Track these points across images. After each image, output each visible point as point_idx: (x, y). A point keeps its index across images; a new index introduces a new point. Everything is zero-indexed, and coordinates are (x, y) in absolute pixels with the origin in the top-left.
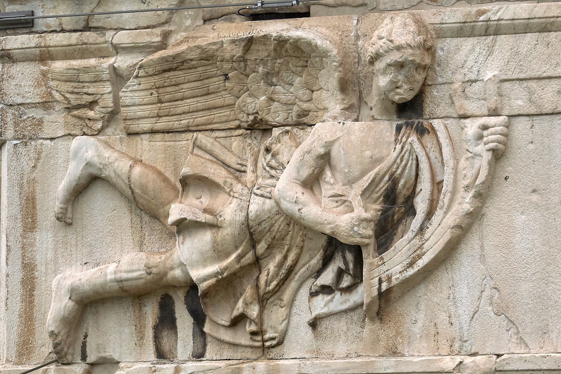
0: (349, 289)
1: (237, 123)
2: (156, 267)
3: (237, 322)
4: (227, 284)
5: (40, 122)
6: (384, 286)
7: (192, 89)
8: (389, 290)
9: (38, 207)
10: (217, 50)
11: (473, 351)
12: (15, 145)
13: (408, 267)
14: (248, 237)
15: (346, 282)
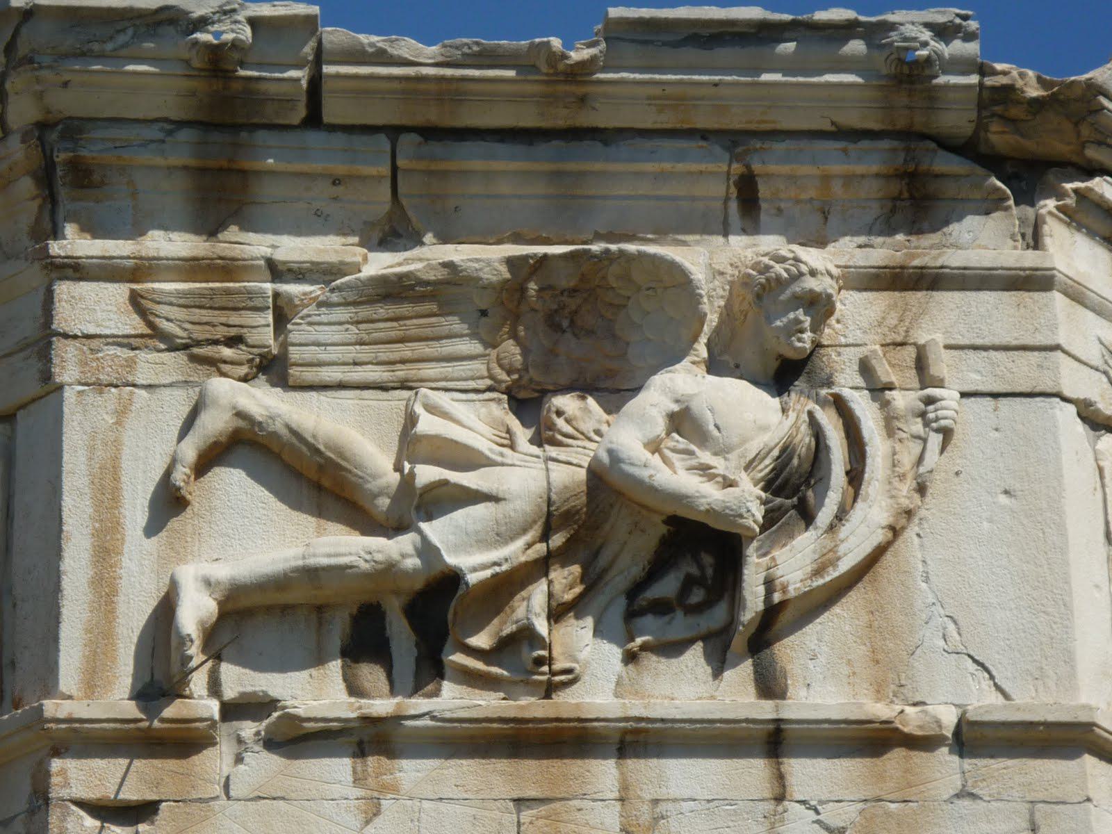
0: (698, 609)
1: (489, 382)
2: (379, 552)
3: (505, 648)
4: (507, 585)
5: (131, 364)
6: (777, 597)
7: (420, 326)
8: (783, 604)
9: (123, 479)
10: (481, 269)
11: (918, 699)
12: (79, 392)
13: (815, 575)
14: (543, 520)
15: (697, 596)
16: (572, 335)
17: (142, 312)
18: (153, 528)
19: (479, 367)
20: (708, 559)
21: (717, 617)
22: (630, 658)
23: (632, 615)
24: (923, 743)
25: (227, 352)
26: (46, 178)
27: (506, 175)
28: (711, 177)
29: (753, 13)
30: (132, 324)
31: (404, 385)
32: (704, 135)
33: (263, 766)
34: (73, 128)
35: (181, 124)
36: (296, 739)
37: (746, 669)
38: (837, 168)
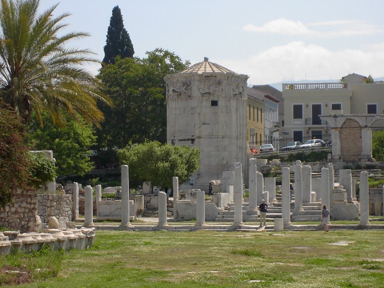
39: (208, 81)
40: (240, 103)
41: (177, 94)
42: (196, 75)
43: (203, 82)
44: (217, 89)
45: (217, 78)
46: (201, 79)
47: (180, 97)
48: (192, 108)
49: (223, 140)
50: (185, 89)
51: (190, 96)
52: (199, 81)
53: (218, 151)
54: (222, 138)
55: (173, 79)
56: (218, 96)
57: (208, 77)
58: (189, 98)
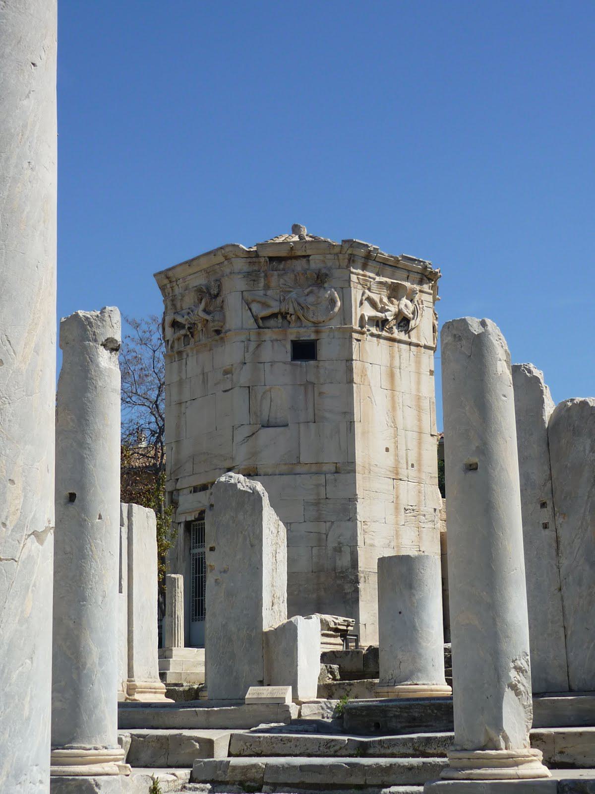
16: (395, 292)
17: (358, 279)
18: (360, 307)
19: (386, 293)
20: (406, 322)
21: (405, 328)
22: (398, 332)
23: (398, 327)
24: (421, 347)
25: (365, 286)
26: (349, 260)
27: (389, 270)
28: (405, 274)
29: (414, 258)
30: (357, 281)
31: (380, 294)
32: (406, 269)
33: (369, 338)
34: (354, 255)
35: (363, 257)
36: (372, 335)
37: (407, 335)
38: (416, 276)
39: (279, 275)
40: (405, 355)
41: (183, 332)
42: (237, 257)
43: (262, 280)
44: (311, 299)
45: (312, 262)
46: (256, 268)
47: (192, 340)
48: (226, 372)
49: (336, 480)
50: (204, 311)
51: (218, 332)
52: (248, 274)
53: (318, 519)
54: (337, 472)
55: (172, 288)
56: (316, 324)
57: (280, 259)
58: (217, 337)
